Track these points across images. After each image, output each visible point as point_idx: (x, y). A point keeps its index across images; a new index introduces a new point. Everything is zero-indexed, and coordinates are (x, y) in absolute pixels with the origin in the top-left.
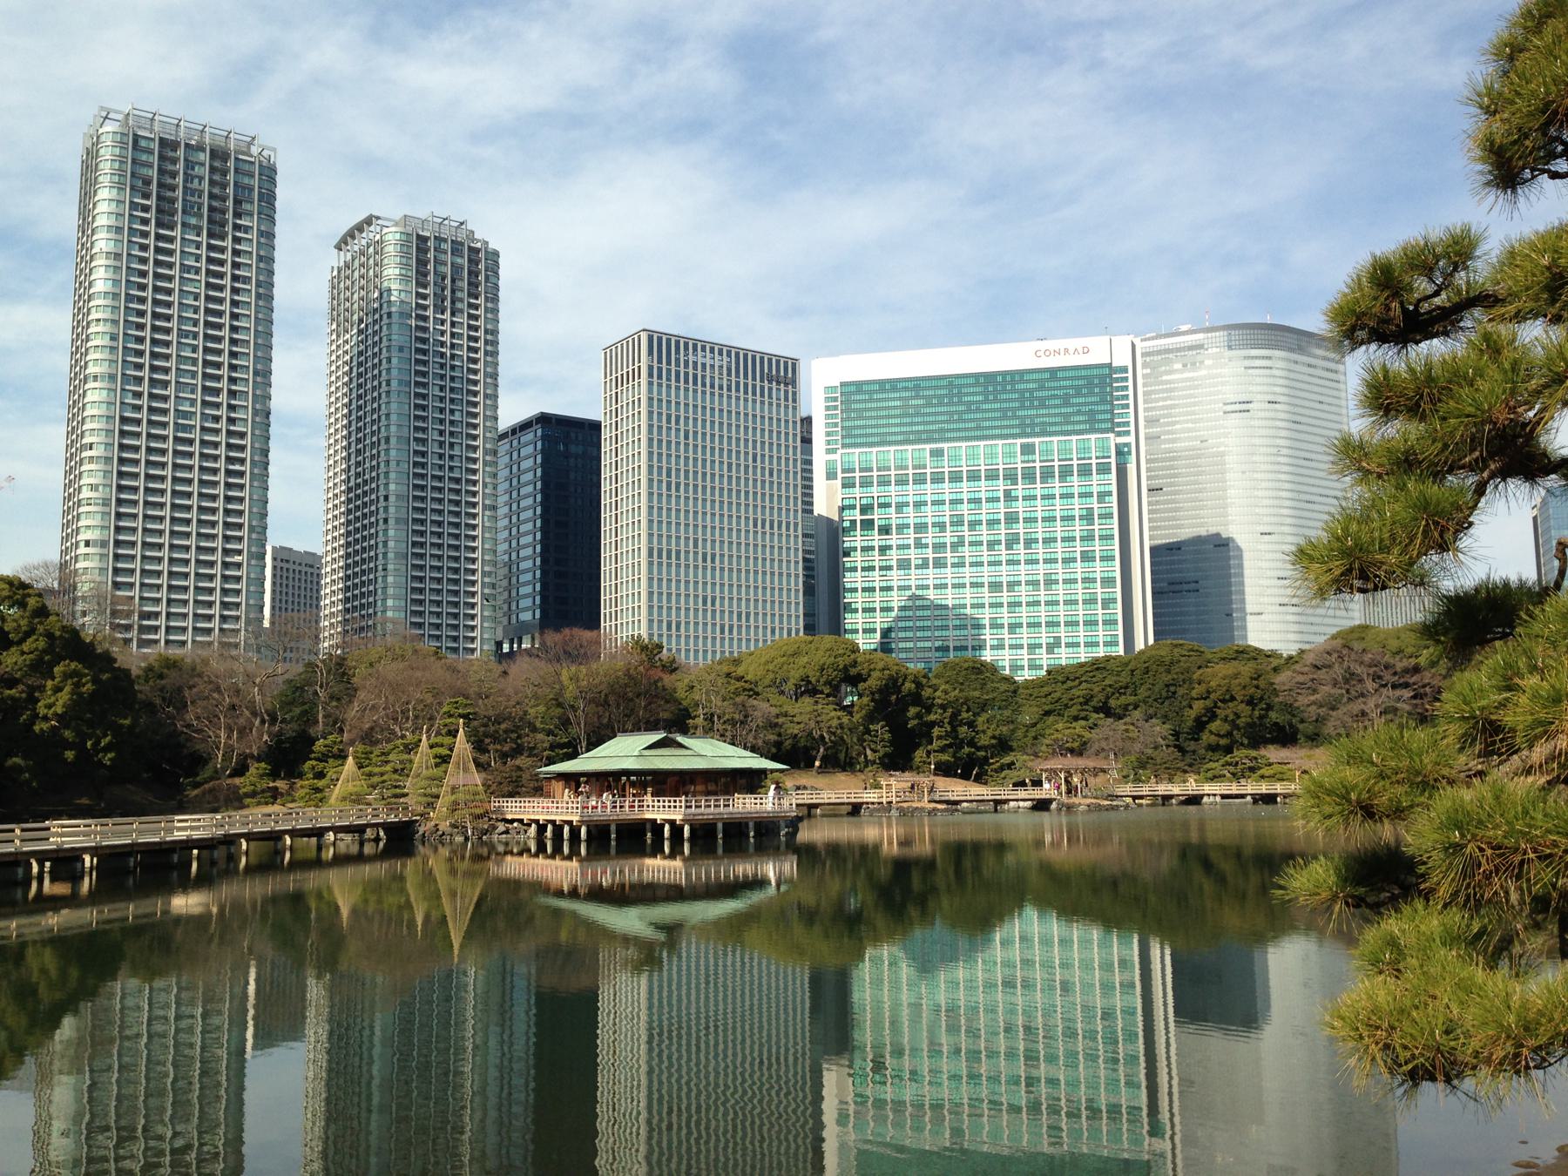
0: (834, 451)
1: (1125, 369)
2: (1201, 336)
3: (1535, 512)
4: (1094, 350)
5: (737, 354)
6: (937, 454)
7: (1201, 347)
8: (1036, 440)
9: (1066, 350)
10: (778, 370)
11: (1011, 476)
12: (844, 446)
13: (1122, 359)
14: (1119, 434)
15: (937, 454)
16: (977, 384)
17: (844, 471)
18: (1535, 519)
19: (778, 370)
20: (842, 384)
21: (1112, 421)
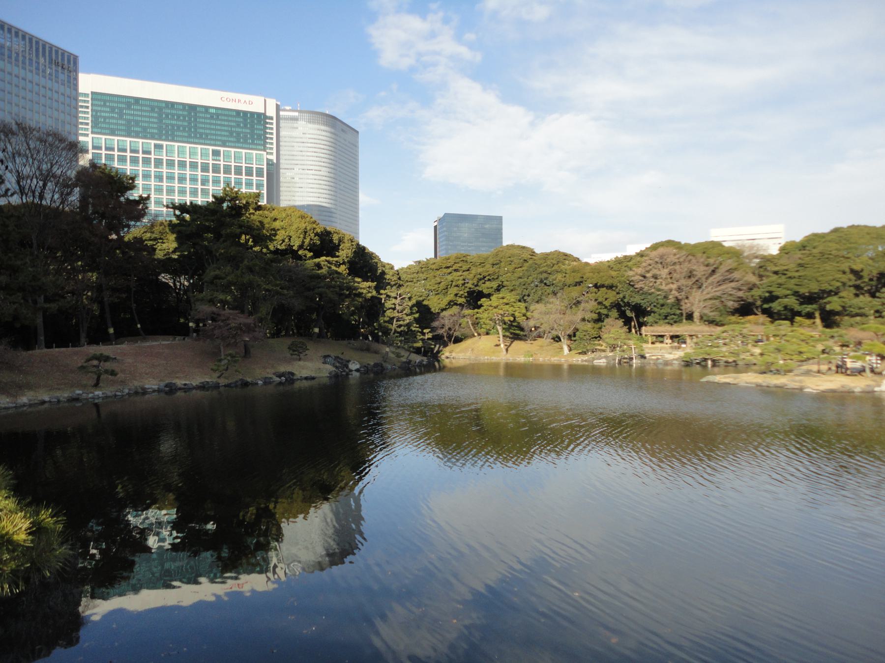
0: (87, 135)
1: (271, 118)
2: (296, 114)
3: (436, 224)
4: (253, 103)
5: (31, 40)
6: (158, 147)
7: (295, 119)
8: (222, 149)
9: (239, 101)
10: (63, 59)
11: (205, 168)
12: (92, 132)
13: (271, 112)
14: (267, 153)
15: (158, 147)
16: (184, 109)
17: (94, 148)
18: (435, 227)
19: (63, 59)
20: (92, 93)
21: (265, 147)
